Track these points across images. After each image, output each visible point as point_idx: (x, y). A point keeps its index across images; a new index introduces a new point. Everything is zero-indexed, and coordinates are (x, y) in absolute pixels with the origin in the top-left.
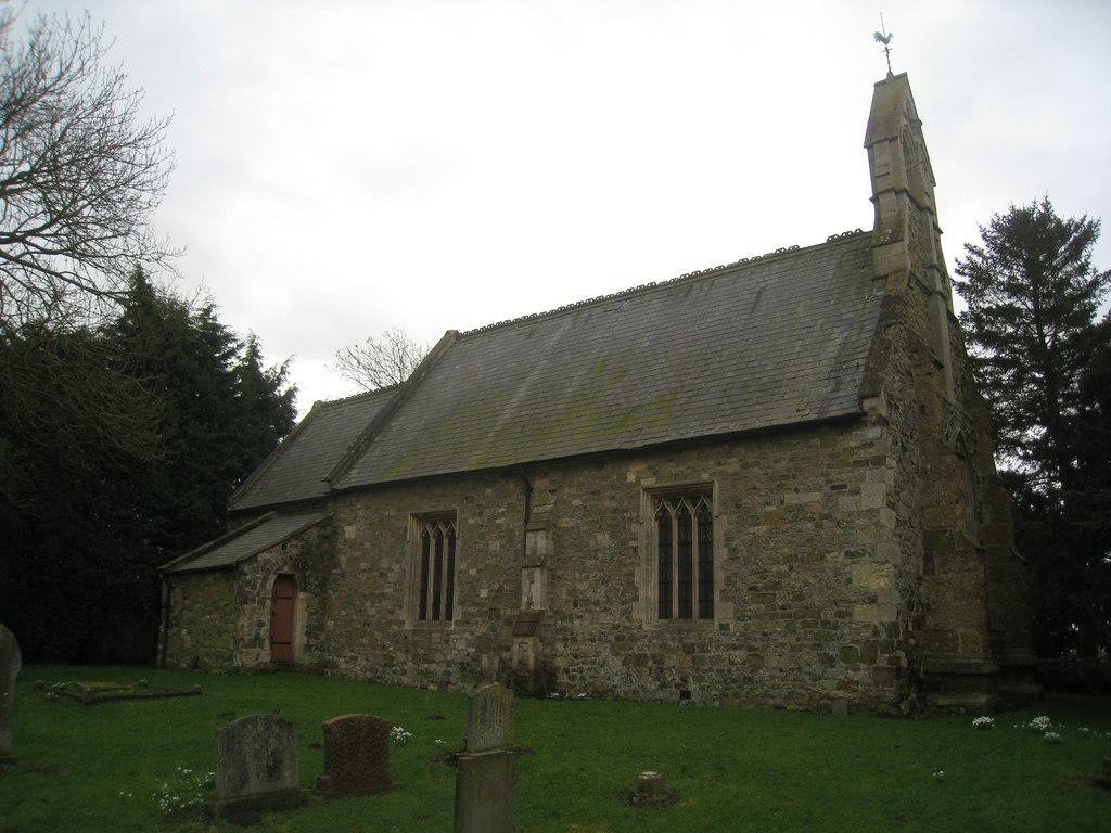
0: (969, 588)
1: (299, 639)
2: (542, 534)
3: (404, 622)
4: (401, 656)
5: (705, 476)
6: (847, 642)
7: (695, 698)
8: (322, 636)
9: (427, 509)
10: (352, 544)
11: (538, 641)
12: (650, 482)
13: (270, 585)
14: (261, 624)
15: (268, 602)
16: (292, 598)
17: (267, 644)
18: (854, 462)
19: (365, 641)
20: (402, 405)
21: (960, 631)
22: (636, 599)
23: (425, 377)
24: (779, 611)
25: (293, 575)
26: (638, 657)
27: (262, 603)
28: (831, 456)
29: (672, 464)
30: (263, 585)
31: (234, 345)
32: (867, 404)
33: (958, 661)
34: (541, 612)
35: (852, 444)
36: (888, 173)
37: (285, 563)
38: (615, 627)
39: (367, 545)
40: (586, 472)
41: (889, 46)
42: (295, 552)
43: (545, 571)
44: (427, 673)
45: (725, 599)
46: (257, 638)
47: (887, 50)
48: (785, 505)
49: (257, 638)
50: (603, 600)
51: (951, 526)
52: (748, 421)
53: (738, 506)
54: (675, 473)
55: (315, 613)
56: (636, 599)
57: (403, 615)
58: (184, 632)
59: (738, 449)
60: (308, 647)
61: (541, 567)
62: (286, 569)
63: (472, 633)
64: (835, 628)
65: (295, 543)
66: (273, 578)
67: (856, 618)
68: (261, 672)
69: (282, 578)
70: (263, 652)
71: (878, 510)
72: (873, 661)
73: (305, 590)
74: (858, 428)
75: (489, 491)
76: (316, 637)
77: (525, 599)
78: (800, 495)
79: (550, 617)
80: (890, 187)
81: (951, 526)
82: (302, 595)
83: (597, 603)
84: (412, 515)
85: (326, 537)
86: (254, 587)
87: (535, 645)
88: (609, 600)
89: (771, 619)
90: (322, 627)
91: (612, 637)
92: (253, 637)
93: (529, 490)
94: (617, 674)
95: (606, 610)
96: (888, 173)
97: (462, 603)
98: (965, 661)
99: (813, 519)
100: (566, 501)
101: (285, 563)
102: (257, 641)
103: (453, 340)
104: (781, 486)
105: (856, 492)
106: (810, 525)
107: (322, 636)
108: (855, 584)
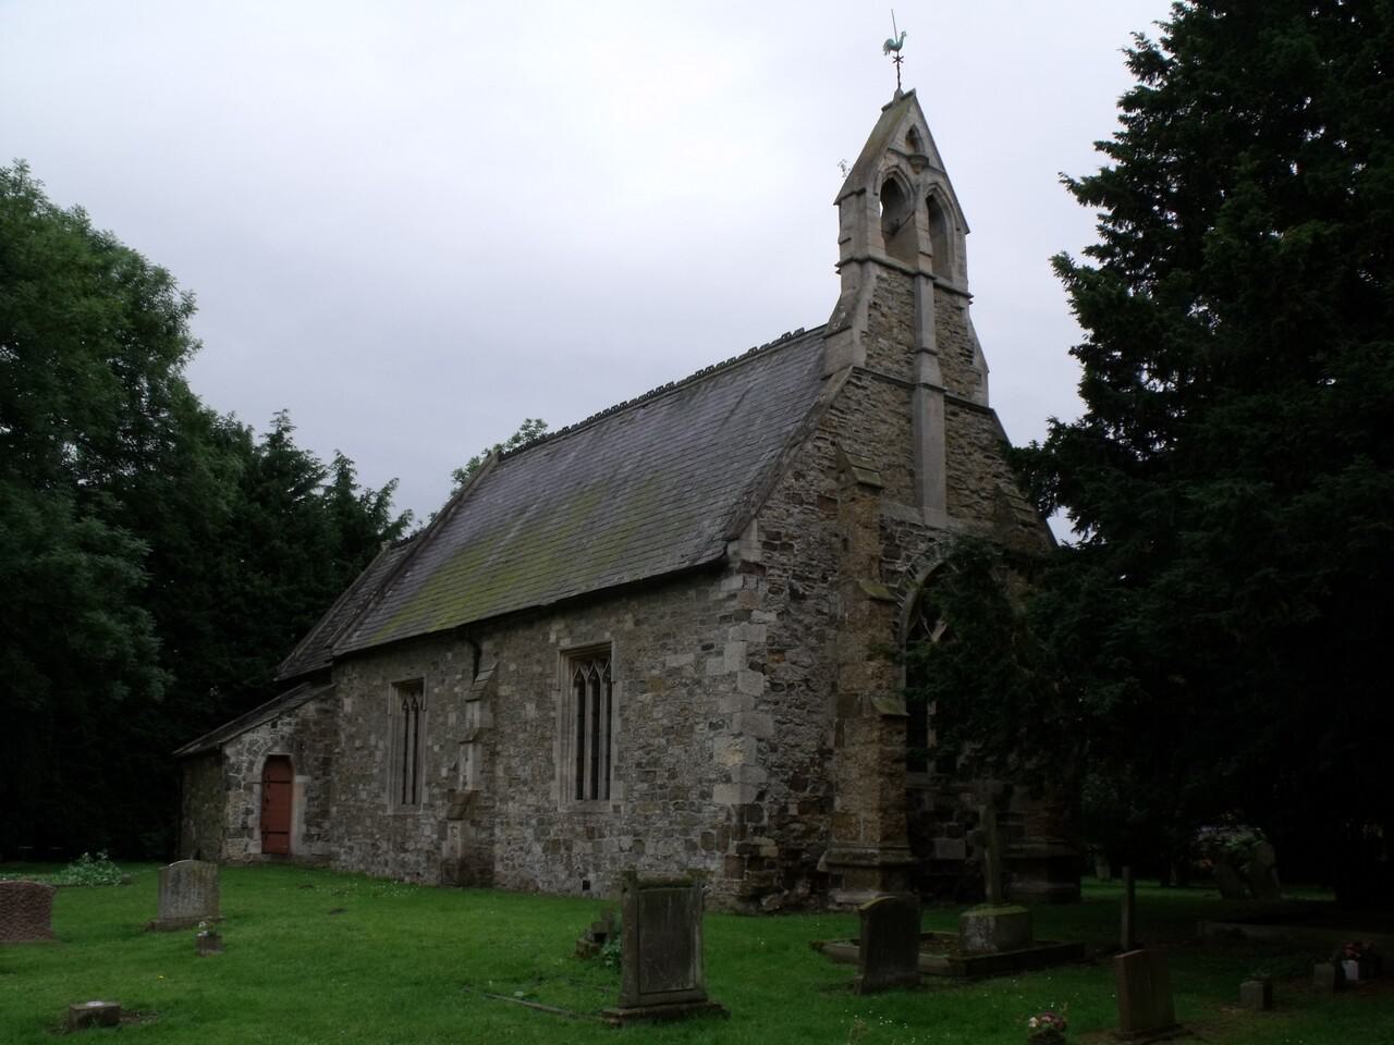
0: (872, 764)
1: (297, 827)
2: (477, 704)
3: (385, 806)
4: (384, 845)
5: (607, 635)
6: (706, 827)
7: (594, 888)
8: (327, 825)
9: (404, 678)
10: (350, 720)
11: (468, 825)
12: (566, 643)
13: (258, 769)
14: (248, 812)
15: (257, 788)
16: (289, 782)
17: (257, 833)
18: (721, 617)
19: (359, 829)
20: (423, 551)
21: (863, 814)
22: (552, 777)
23: (455, 514)
24: (658, 791)
25: (288, 757)
26: (557, 842)
27: (249, 788)
28: (704, 610)
29: (583, 622)
30: (250, 769)
31: (80, 537)
32: (732, 548)
33: (858, 851)
34: (475, 793)
35: (721, 596)
36: (849, 239)
37: (276, 744)
38: (538, 810)
39: (360, 720)
40: (520, 632)
41: (901, 53)
42: (287, 730)
43: (480, 747)
44: (403, 864)
45: (620, 777)
46: (245, 827)
47: (898, 59)
48: (666, 669)
49: (245, 827)
50: (530, 779)
51: (861, 689)
52: (638, 571)
53: (631, 670)
54: (591, 631)
55: (317, 798)
56: (552, 777)
57: (385, 799)
58: (192, 822)
59: (633, 603)
60: (308, 837)
61: (474, 741)
62: (277, 751)
63: (436, 818)
64: (699, 811)
65: (288, 720)
66: (260, 761)
67: (716, 799)
68: (252, 865)
69: (272, 761)
70: (252, 843)
71: (735, 675)
72: (726, 848)
73: (302, 772)
74: (726, 577)
75: (450, 655)
76: (319, 825)
77: (461, 778)
78: (678, 656)
79: (487, 798)
80: (849, 257)
81: (861, 689)
82: (298, 779)
83: (525, 783)
84: (394, 685)
85: (327, 711)
86: (238, 771)
87: (464, 831)
88: (534, 780)
89: (652, 799)
90: (325, 813)
91: (534, 822)
92: (239, 826)
93: (478, 654)
94: (538, 862)
95: (532, 790)
96: (849, 239)
97: (428, 784)
98: (864, 851)
99: (686, 685)
100: (506, 660)
101: (276, 744)
102: (245, 830)
103: (494, 462)
104: (664, 647)
105: (720, 653)
106: (684, 691)
107: (327, 825)
108: (716, 760)
